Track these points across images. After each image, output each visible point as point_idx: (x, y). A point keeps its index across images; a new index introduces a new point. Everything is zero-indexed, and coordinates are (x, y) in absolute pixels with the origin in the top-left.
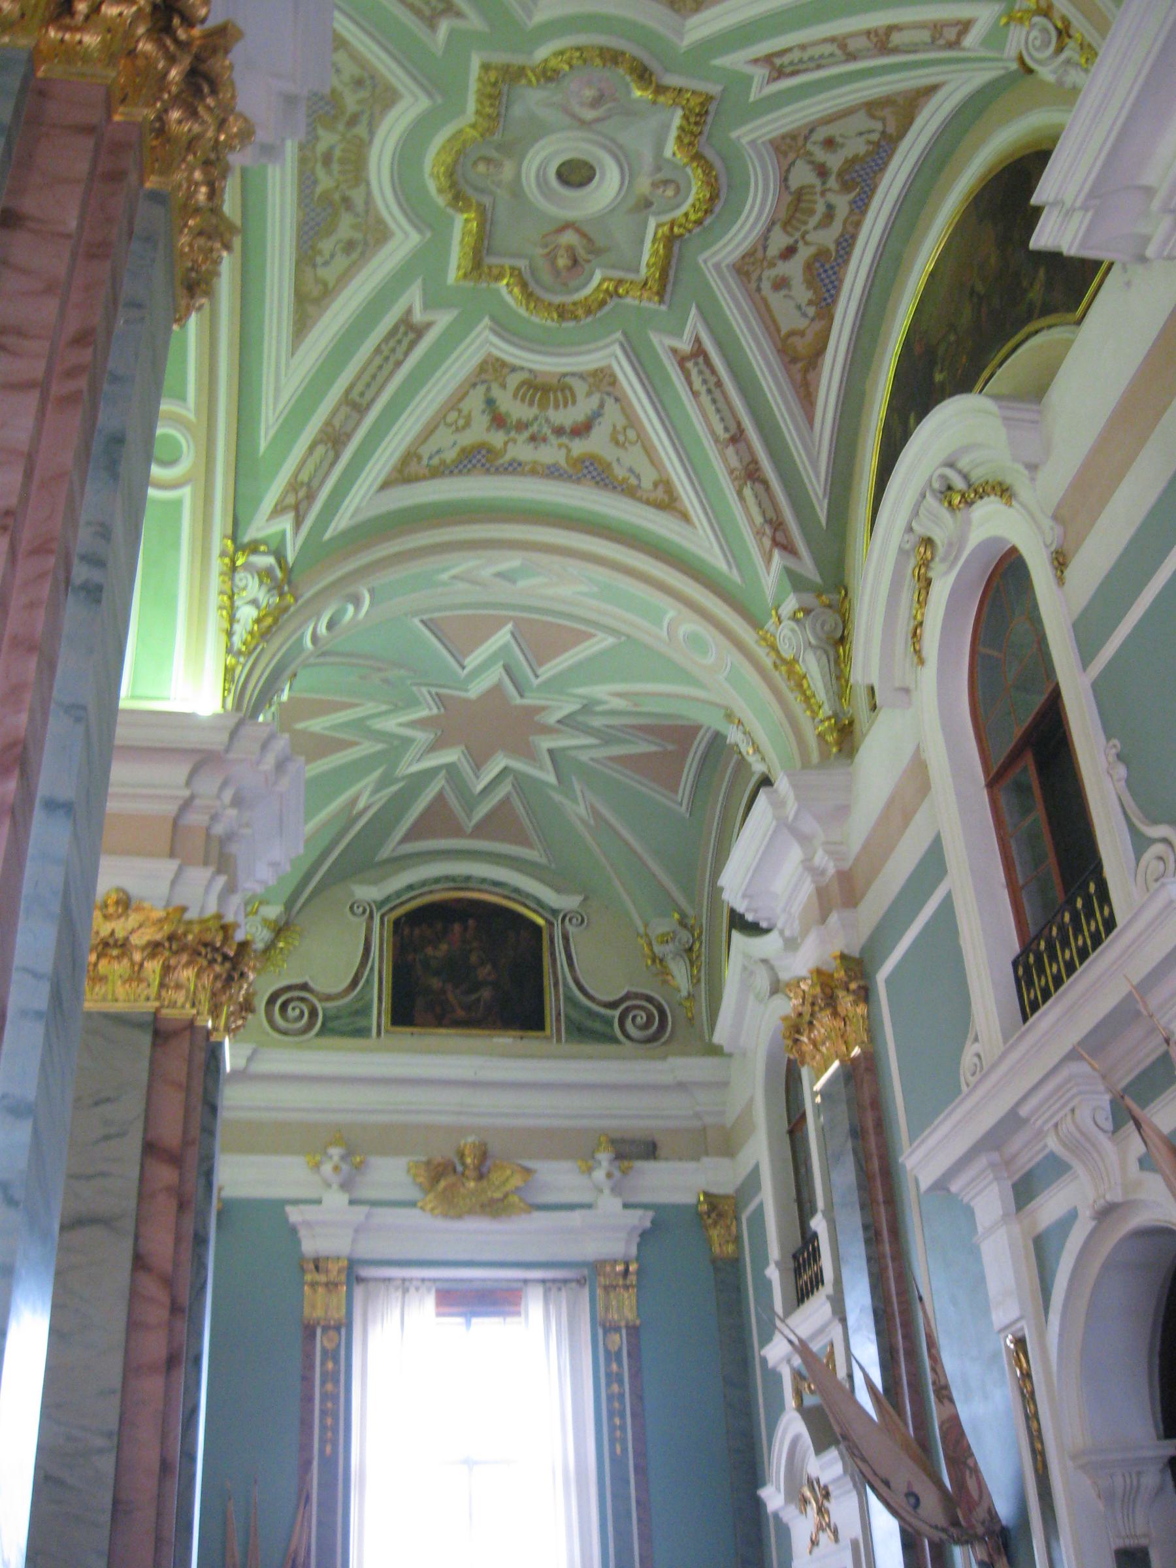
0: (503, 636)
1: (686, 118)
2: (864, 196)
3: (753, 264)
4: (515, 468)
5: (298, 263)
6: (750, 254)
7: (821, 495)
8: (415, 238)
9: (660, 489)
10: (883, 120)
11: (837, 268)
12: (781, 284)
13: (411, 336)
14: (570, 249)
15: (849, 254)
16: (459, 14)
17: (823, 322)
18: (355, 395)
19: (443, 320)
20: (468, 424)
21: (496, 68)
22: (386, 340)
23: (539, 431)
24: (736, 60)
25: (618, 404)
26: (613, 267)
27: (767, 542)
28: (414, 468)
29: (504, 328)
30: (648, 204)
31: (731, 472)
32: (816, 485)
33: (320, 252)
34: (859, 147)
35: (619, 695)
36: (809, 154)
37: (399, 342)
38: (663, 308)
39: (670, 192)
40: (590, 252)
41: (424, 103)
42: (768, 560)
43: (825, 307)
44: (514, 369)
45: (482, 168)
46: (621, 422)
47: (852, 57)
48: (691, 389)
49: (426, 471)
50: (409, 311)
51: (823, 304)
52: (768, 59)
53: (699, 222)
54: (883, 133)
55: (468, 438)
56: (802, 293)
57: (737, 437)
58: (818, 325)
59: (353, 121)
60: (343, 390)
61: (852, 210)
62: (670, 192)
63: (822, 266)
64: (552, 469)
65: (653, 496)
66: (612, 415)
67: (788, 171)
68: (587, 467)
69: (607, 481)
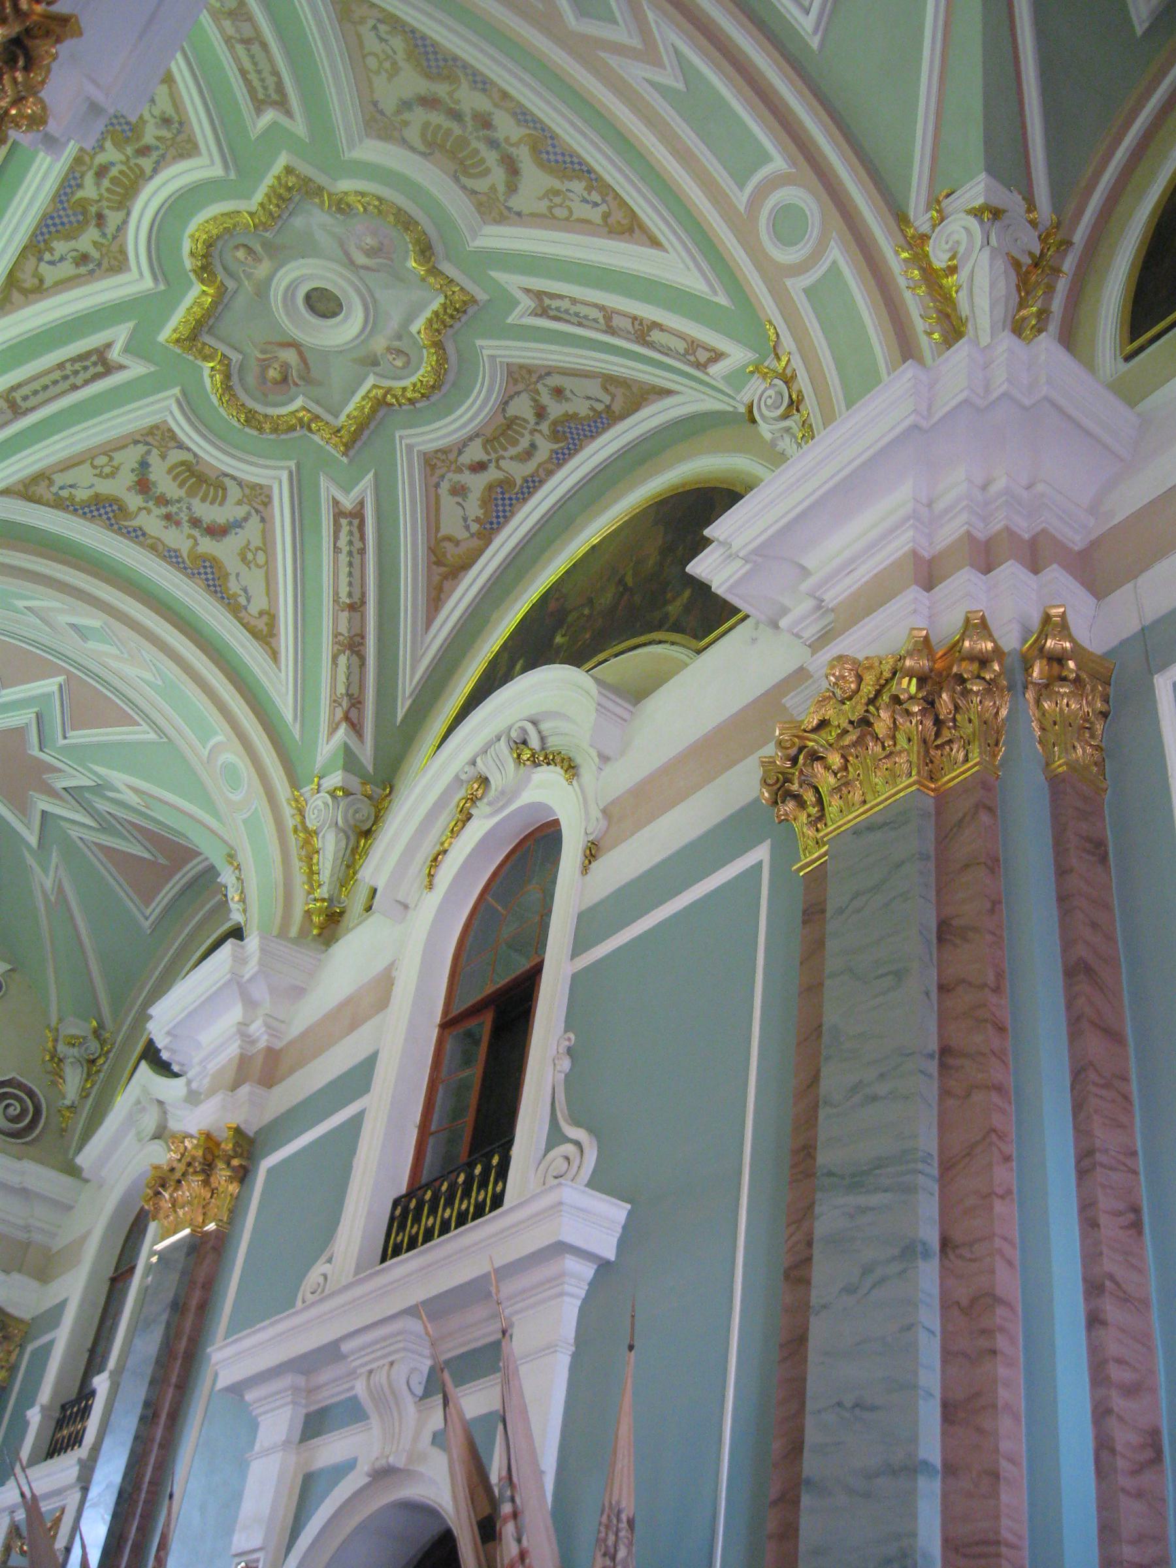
0: (50, 685)
1: (444, 306)
2: (566, 451)
3: (443, 461)
4: (137, 535)
5: (25, 248)
6: (444, 451)
7: (407, 694)
8: (148, 283)
9: (265, 619)
10: (613, 397)
11: (514, 502)
12: (459, 491)
13: (100, 369)
14: (285, 367)
15: (531, 494)
16: (289, 113)
17: (481, 543)
18: (18, 395)
19: (137, 369)
20: (112, 475)
21: (298, 176)
22: (73, 360)
24: (512, 282)
26: (318, 402)
27: (339, 714)
28: (41, 490)
29: (190, 404)
30: (375, 363)
31: (336, 635)
32: (408, 682)
33: (51, 250)
34: (582, 408)
35: (136, 790)
36: (537, 392)
37: (86, 368)
38: (345, 460)
40: (302, 378)
41: (217, 171)
42: (333, 730)
43: (489, 529)
44: (181, 446)
45: (241, 254)
46: (257, 542)
47: (611, 330)
49: (52, 498)
50: (109, 346)
51: (488, 526)
52: (539, 295)
53: (412, 402)
54: (608, 407)
55: (106, 487)
56: (474, 508)
57: (356, 607)
58: (476, 543)
59: (144, 151)
60: (9, 385)
63: (503, 493)
64: (172, 554)
65: (253, 622)
66: (252, 530)
67: (511, 397)
68: (205, 567)
69: (218, 589)
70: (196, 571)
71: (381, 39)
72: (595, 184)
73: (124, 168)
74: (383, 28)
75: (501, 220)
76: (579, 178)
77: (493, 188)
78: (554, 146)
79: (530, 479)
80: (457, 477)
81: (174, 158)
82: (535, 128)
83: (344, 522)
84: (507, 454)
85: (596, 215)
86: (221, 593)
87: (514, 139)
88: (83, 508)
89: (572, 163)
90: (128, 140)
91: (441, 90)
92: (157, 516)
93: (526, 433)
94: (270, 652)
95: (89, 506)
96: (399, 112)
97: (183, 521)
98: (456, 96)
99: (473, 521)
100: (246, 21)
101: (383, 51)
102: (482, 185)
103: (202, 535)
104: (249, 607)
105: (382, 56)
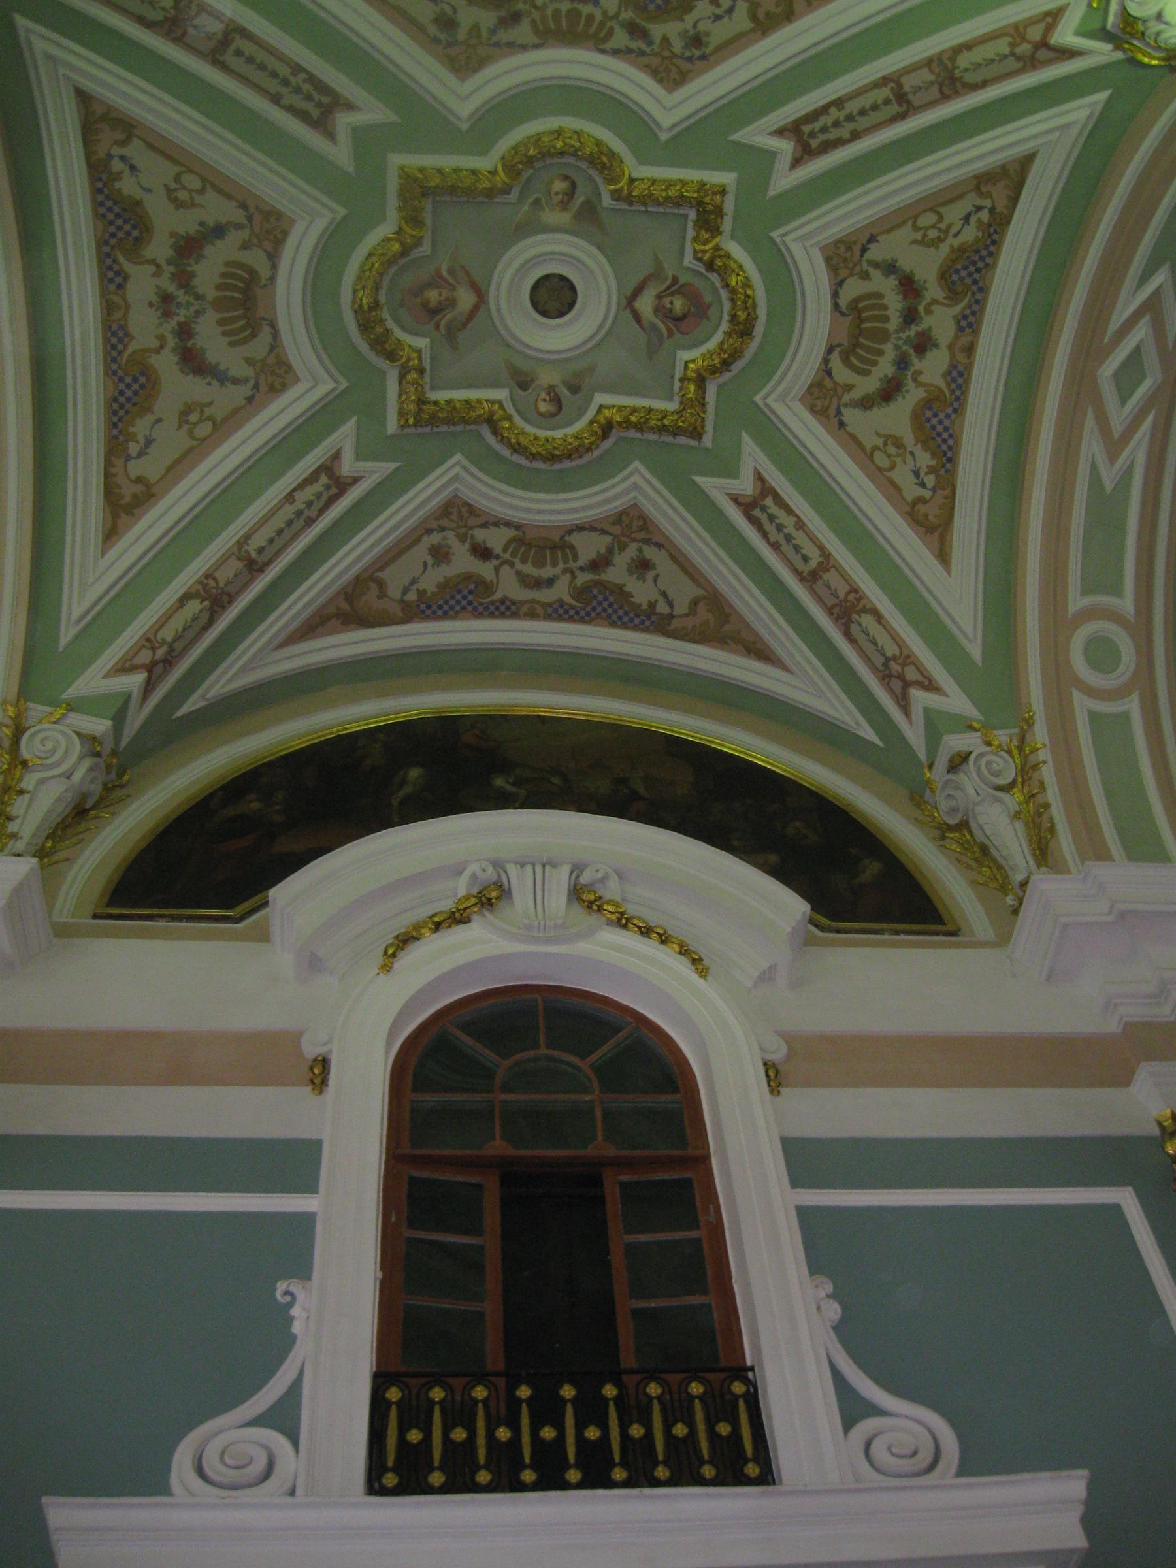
2: (572, 612)
3: (461, 517)
6: (472, 510)
9: (138, 489)
11: (470, 608)
12: (440, 554)
13: (315, 113)
14: (452, 303)
15: (492, 615)
16: (796, 163)
17: (400, 614)
18: (239, 42)
19: (341, 153)
20: (179, 204)
21: (722, 201)
22: (312, 79)
23: (179, 305)
25: (244, 402)
30: (523, 385)
36: (623, 548)
37: (309, 98)
39: (543, 407)
40: (449, 327)
42: (124, 667)
44: (273, 258)
45: (559, 186)
46: (219, 413)
48: (295, 490)
50: (350, 107)
51: (423, 606)
55: (159, 210)
56: (431, 581)
57: (254, 567)
58: (396, 610)
59: (634, 30)
61: (550, 605)
62: (543, 407)
63: (470, 592)
64: (121, 334)
66: (225, 398)
67: (593, 529)
69: (121, 413)
70: (120, 373)
71: (966, 219)
72: (942, 472)
73: (599, 17)
74: (985, 216)
75: (820, 413)
76: (934, 455)
77: (849, 387)
78: (948, 416)
79: (508, 603)
80: (451, 538)
81: (647, 66)
82: (952, 392)
83: (324, 479)
84: (519, 566)
85: (911, 491)
86: (120, 420)
87: (921, 379)
88: (107, 197)
89: (945, 441)
90: (642, 9)
91: (934, 291)
92: (157, 287)
93: (561, 566)
94: (109, 525)
95: (115, 203)
96: (876, 265)
97: (176, 318)
98: (934, 308)
99: (418, 590)
100: (941, 92)
101: (949, 227)
102: (842, 374)
103: (174, 350)
104: (133, 461)
105: (943, 226)
